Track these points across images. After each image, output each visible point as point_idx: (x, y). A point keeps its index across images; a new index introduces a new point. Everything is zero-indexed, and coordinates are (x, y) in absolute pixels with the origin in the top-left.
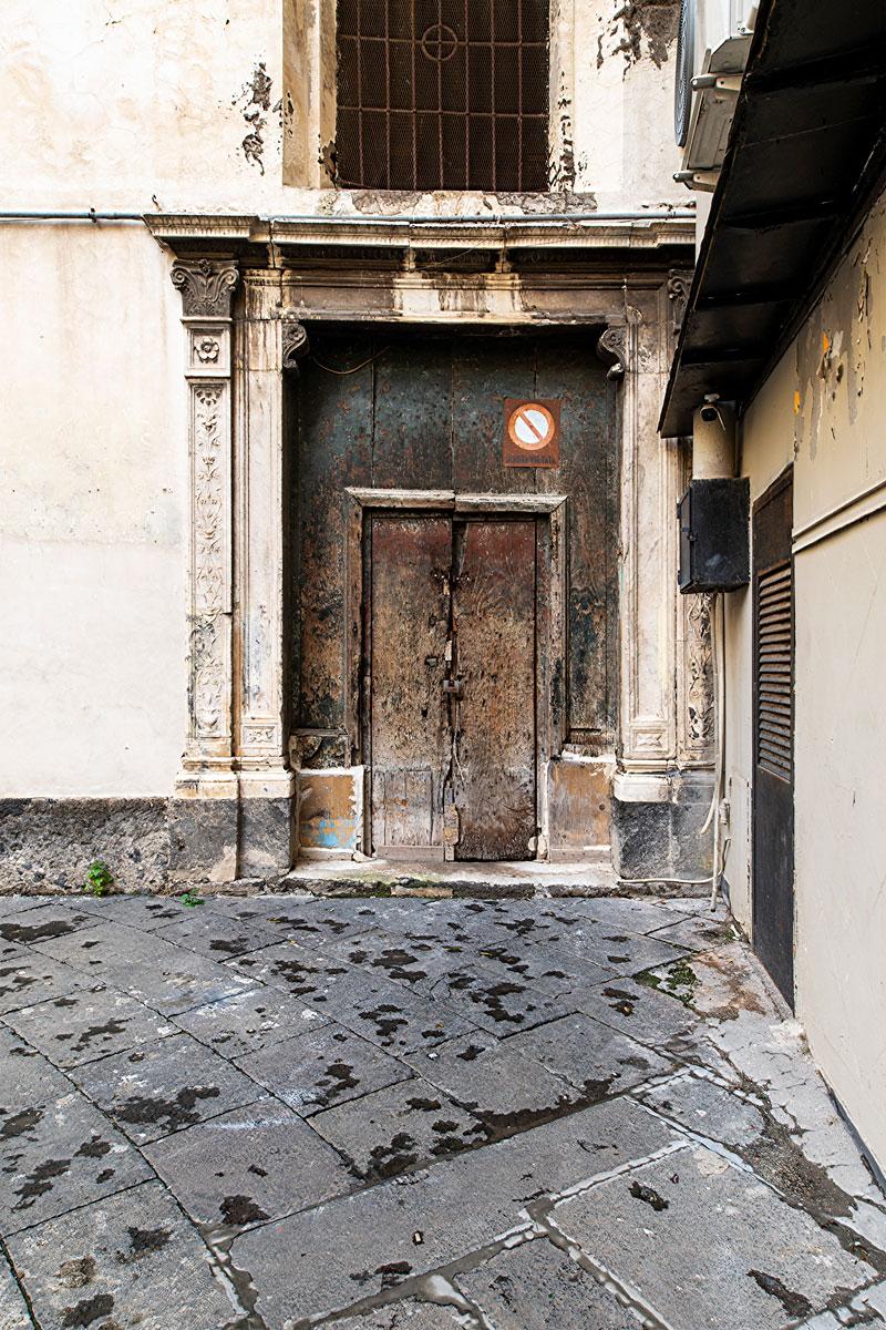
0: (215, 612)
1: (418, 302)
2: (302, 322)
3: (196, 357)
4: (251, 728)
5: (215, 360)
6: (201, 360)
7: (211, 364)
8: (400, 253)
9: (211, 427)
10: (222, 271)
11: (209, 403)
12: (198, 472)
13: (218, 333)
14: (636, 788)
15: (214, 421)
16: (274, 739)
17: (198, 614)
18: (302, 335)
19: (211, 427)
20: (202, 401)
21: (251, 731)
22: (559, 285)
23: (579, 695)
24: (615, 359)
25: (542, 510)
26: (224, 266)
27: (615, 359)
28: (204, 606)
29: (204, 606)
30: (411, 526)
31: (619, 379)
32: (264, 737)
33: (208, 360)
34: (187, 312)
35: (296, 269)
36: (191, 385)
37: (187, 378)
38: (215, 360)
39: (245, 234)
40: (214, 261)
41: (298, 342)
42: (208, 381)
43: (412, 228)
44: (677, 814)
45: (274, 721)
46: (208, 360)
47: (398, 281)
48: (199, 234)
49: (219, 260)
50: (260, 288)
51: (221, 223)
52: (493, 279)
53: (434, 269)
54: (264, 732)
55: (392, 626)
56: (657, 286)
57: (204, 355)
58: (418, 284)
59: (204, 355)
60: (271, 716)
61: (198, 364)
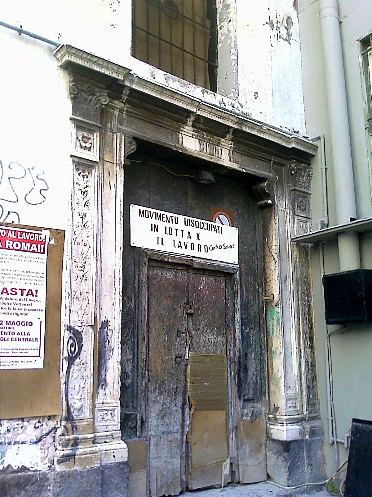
0: (84, 324)
1: (190, 143)
2: (134, 138)
3: (78, 144)
4: (101, 411)
5: (89, 149)
6: (81, 147)
7: (87, 152)
8: (188, 113)
9: (84, 192)
10: (98, 95)
11: (83, 177)
12: (75, 223)
13: (92, 132)
14: (283, 432)
15: (86, 189)
16: (116, 418)
17: (73, 325)
18: (134, 146)
19: (84, 192)
20: (79, 174)
21: (101, 413)
22: (247, 153)
23: (250, 378)
24: (268, 196)
25: (231, 271)
26: (101, 92)
27: (268, 196)
28: (76, 319)
29: (76, 319)
30: (169, 273)
31: (270, 207)
32: (109, 417)
33: (85, 147)
34: (74, 111)
35: (134, 105)
36: (74, 161)
37: (71, 156)
38: (89, 149)
39: (121, 78)
40: (91, 84)
41: (132, 150)
42: (84, 162)
43: (200, 104)
44: (309, 444)
45: (116, 405)
46: (85, 147)
47: (182, 129)
48: (96, 68)
49: (97, 87)
50: (112, 111)
51: (110, 66)
52: (223, 142)
53: (199, 128)
54: (109, 413)
55: (159, 336)
56: (283, 165)
57: (84, 145)
58: (190, 134)
59: (84, 145)
60: (113, 401)
61: (79, 148)
